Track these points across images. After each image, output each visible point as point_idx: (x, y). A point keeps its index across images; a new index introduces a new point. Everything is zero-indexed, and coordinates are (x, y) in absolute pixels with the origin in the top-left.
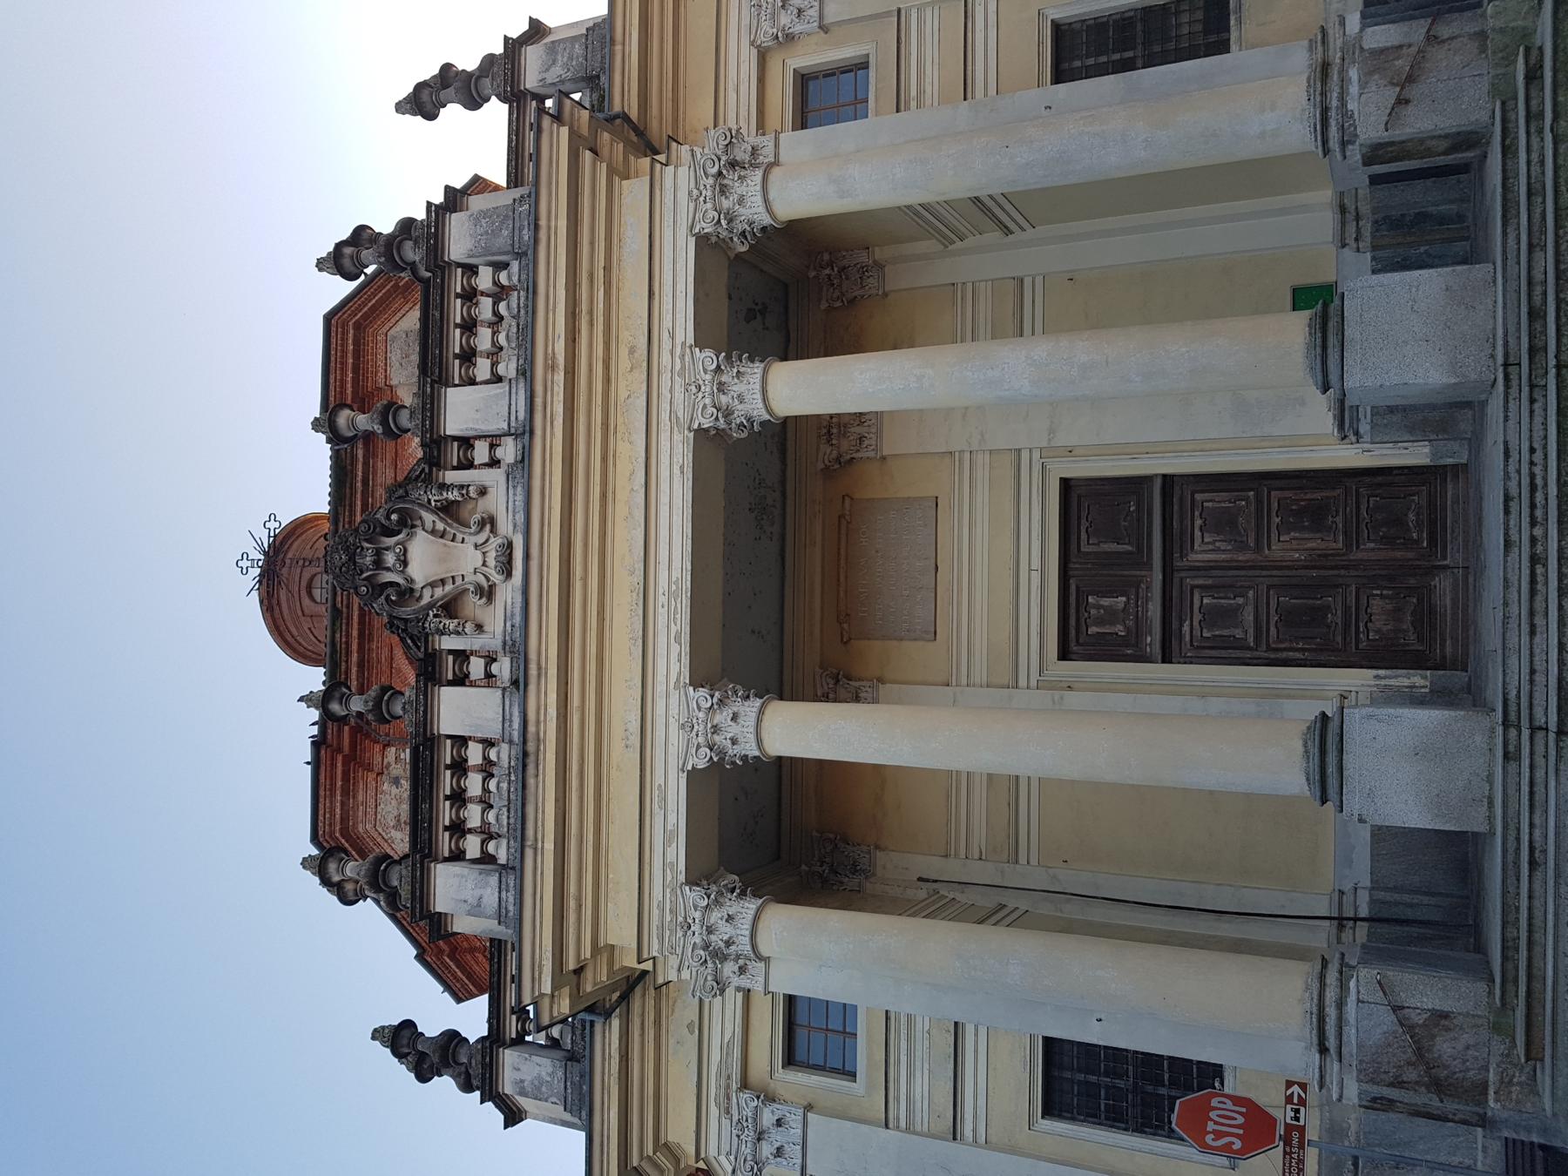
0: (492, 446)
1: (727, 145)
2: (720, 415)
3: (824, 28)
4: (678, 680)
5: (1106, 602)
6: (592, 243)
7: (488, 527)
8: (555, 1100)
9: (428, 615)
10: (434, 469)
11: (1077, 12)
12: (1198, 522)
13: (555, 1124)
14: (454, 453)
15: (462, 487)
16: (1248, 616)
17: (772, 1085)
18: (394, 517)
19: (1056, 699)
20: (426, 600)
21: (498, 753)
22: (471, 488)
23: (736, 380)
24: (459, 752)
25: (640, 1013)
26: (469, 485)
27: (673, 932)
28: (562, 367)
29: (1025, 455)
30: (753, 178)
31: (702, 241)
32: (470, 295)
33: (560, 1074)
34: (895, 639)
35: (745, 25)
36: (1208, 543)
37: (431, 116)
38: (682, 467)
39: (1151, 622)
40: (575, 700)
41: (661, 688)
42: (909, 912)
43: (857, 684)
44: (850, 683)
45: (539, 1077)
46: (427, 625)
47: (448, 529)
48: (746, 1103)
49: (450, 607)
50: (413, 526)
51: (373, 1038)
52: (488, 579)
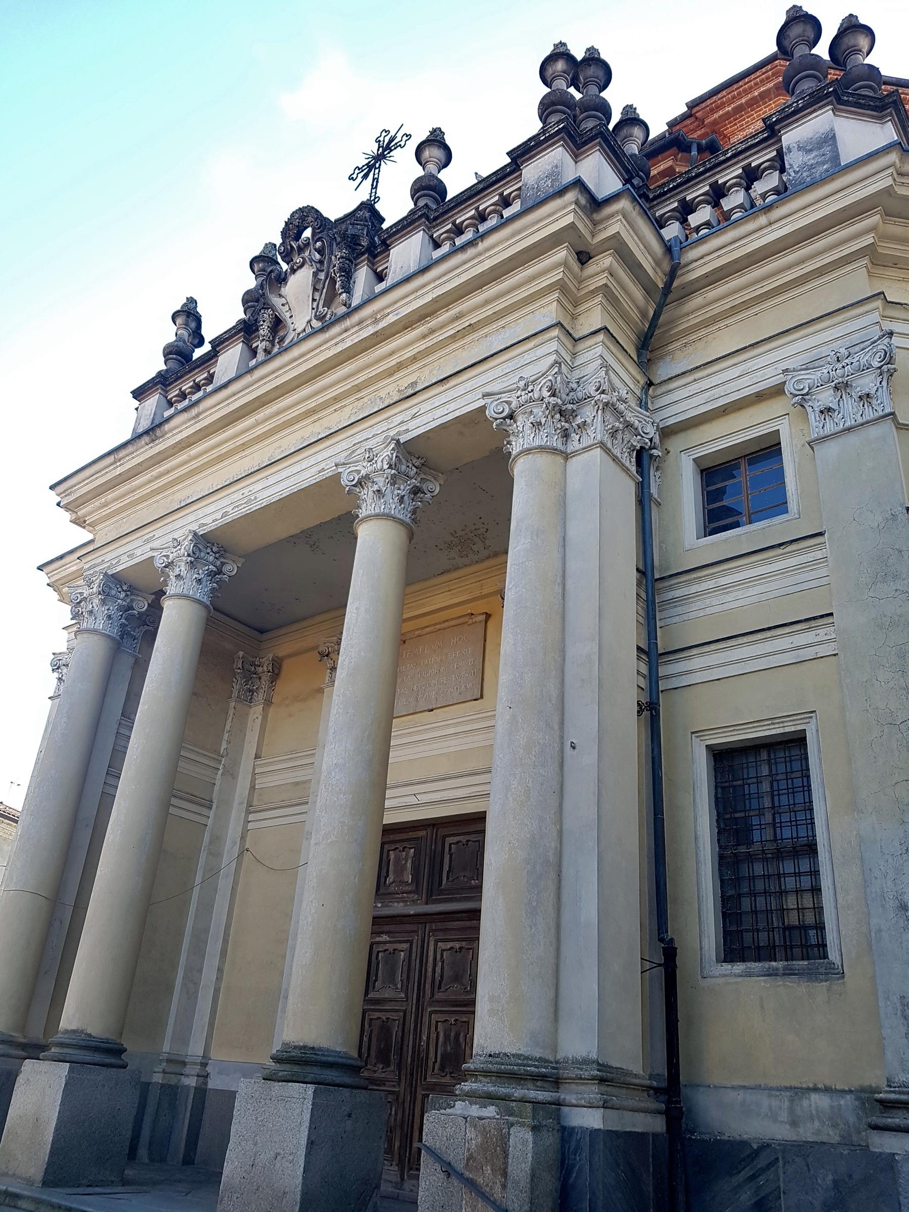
6: (487, 302)
16: (387, 994)
35: (821, 352)
36: (442, 955)
38: (323, 470)
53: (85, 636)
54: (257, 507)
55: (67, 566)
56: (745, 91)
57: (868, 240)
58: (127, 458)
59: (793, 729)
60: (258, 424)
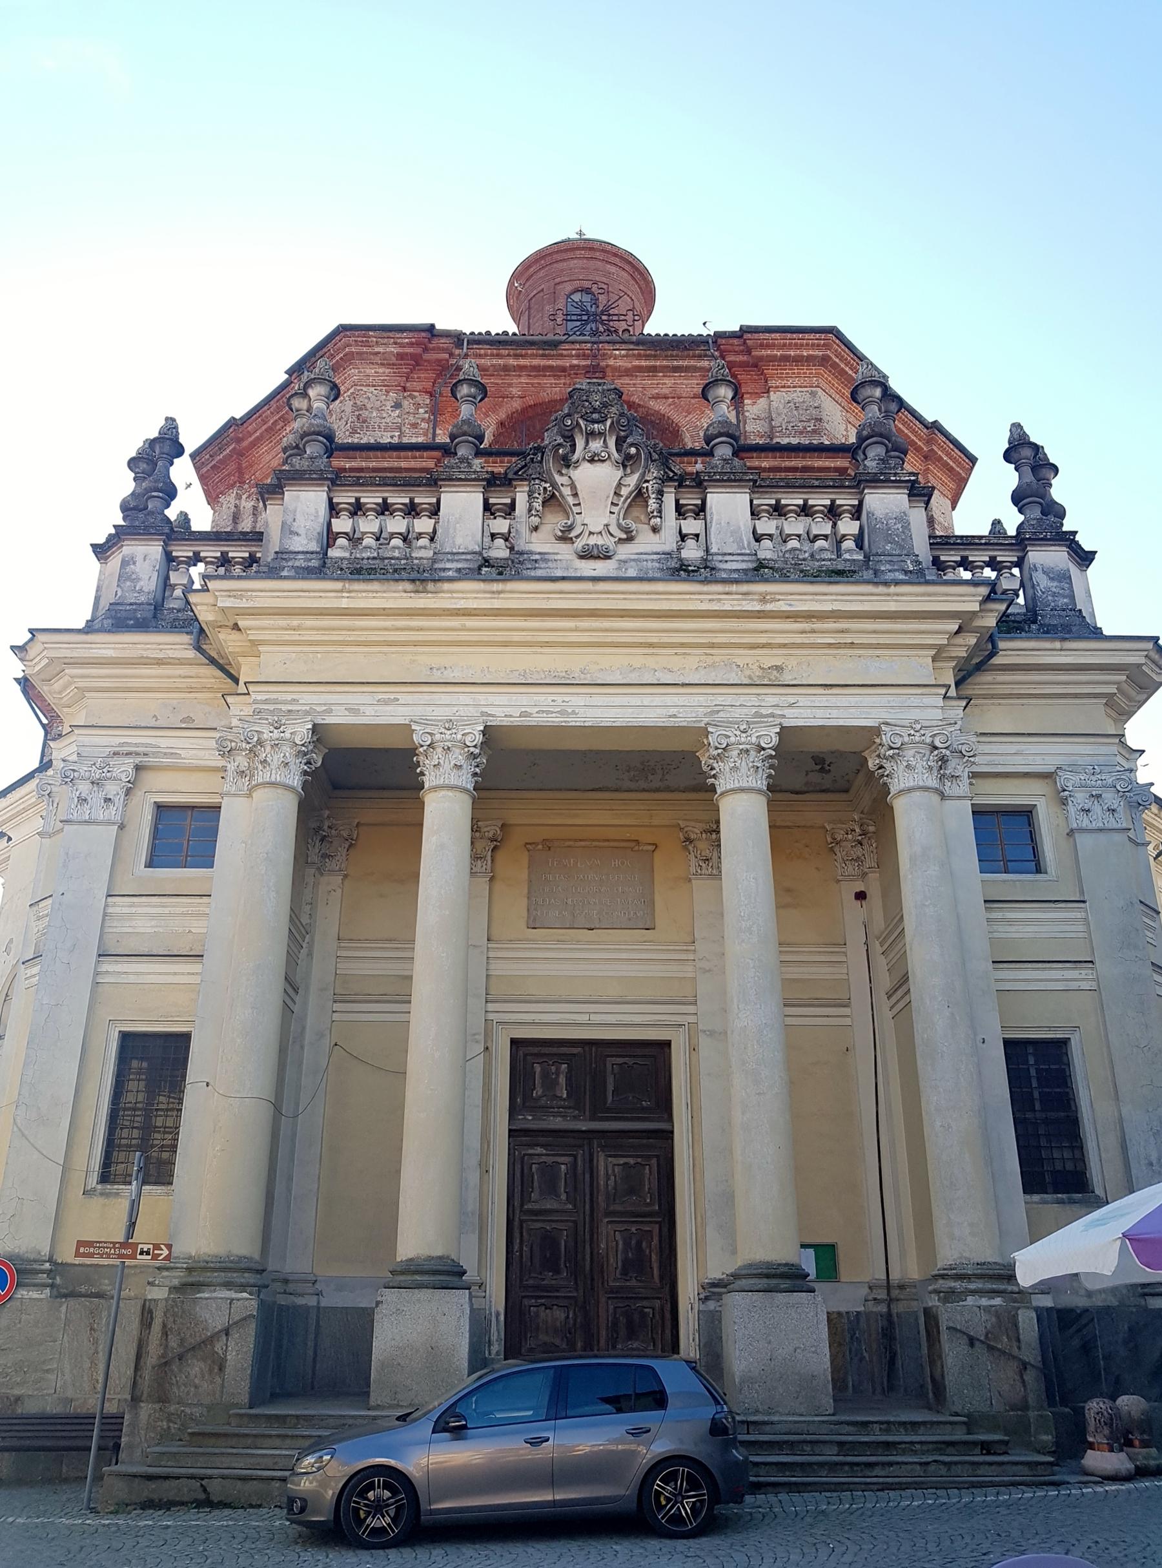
0: (697, 536)
1: (961, 752)
2: (720, 751)
3: (1071, 833)
4: (490, 715)
5: (562, 1080)
7: (624, 536)
8: (119, 594)
9: (546, 482)
10: (676, 484)
11: (1076, 1061)
12: (632, 1161)
13: (97, 591)
14: (691, 500)
15: (660, 512)
16: (549, 1204)
17: (140, 793)
18: (633, 450)
19: (477, 1037)
20: (559, 480)
21: (425, 548)
22: (658, 519)
23: (751, 764)
24: (425, 510)
25: (200, 675)
26: (661, 517)
27: (272, 712)
28: (763, 608)
29: (691, 1009)
30: (930, 778)
31: (876, 731)
32: (833, 512)
33: (143, 599)
34: (529, 892)
35: (1077, 761)
37: (1008, 456)
38: (674, 716)
39: (544, 1120)
40: (471, 622)
41: (482, 699)
42: (293, 916)
43: (489, 858)
44: (490, 852)
45: (138, 579)
46: (537, 481)
47: (622, 499)
48: (124, 769)
49: (551, 500)
50: (625, 466)
51: (167, 419)
52: (577, 537)
53: (279, 791)
54: (578, 724)
55: (93, 646)
56: (796, 344)
57: (1113, 689)
58: (364, 594)
59: (1061, 1036)
60: (576, 630)
